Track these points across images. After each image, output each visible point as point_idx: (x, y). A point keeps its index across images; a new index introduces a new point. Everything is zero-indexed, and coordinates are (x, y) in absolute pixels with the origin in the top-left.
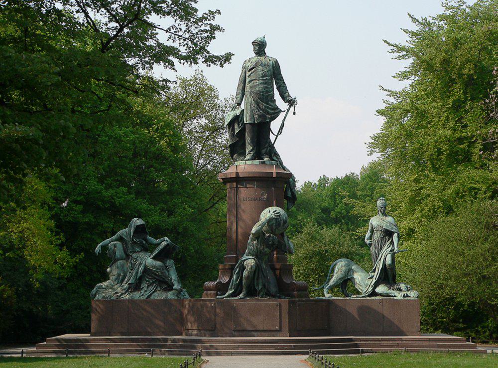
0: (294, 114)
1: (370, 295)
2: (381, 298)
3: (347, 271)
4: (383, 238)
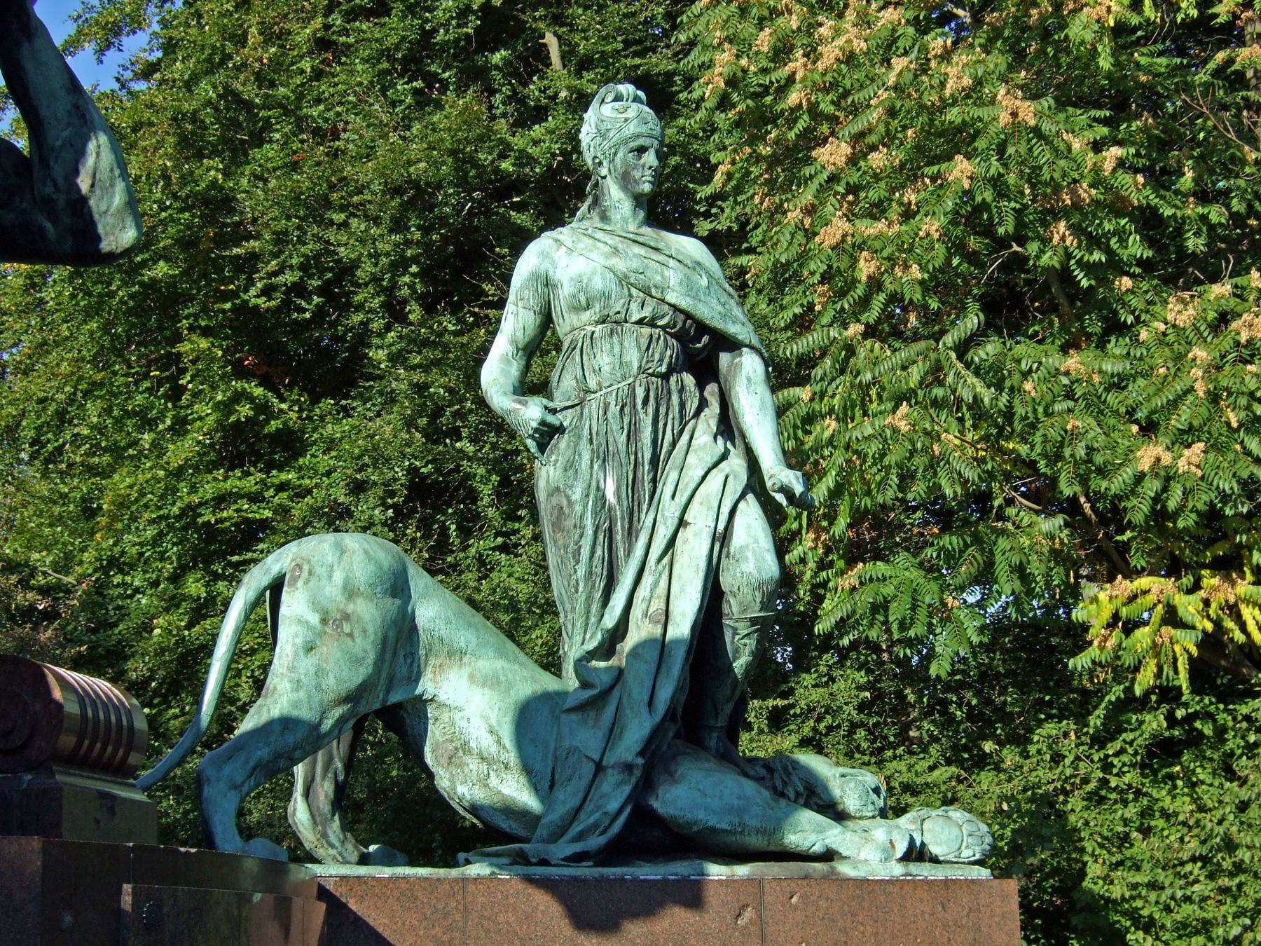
1: (614, 853)
2: (742, 870)
3: (391, 634)
4: (666, 377)
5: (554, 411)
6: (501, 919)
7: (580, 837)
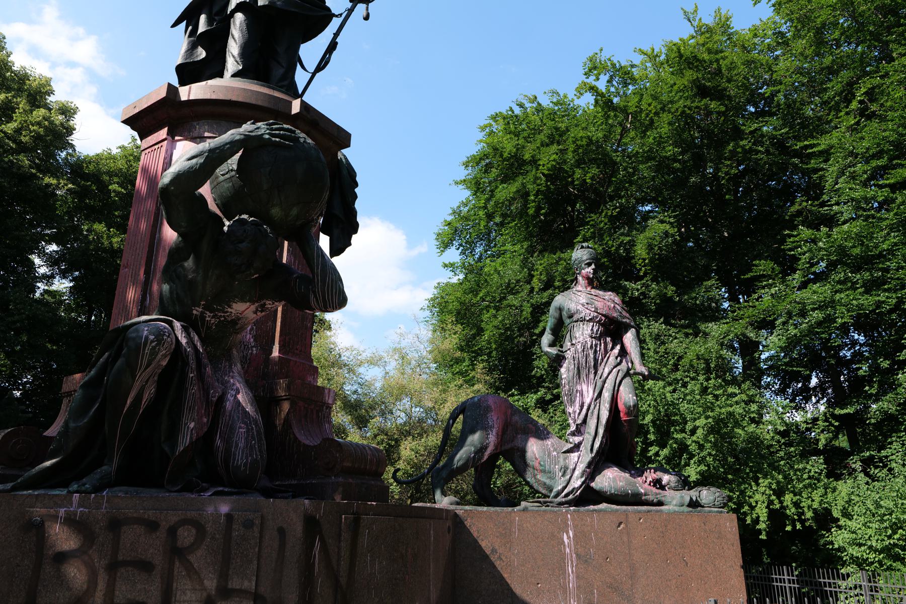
0: (367, 18)
5: (562, 352)
6: (525, 525)
7: (567, 495)
